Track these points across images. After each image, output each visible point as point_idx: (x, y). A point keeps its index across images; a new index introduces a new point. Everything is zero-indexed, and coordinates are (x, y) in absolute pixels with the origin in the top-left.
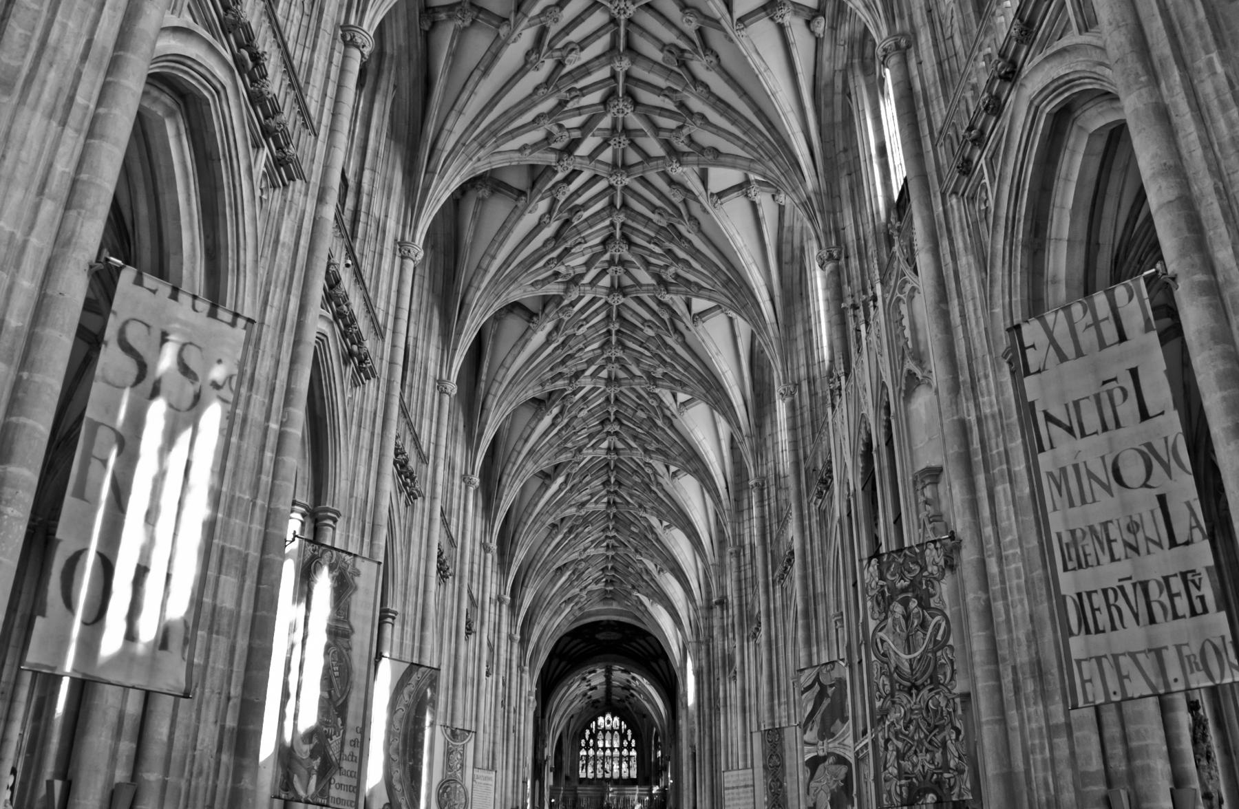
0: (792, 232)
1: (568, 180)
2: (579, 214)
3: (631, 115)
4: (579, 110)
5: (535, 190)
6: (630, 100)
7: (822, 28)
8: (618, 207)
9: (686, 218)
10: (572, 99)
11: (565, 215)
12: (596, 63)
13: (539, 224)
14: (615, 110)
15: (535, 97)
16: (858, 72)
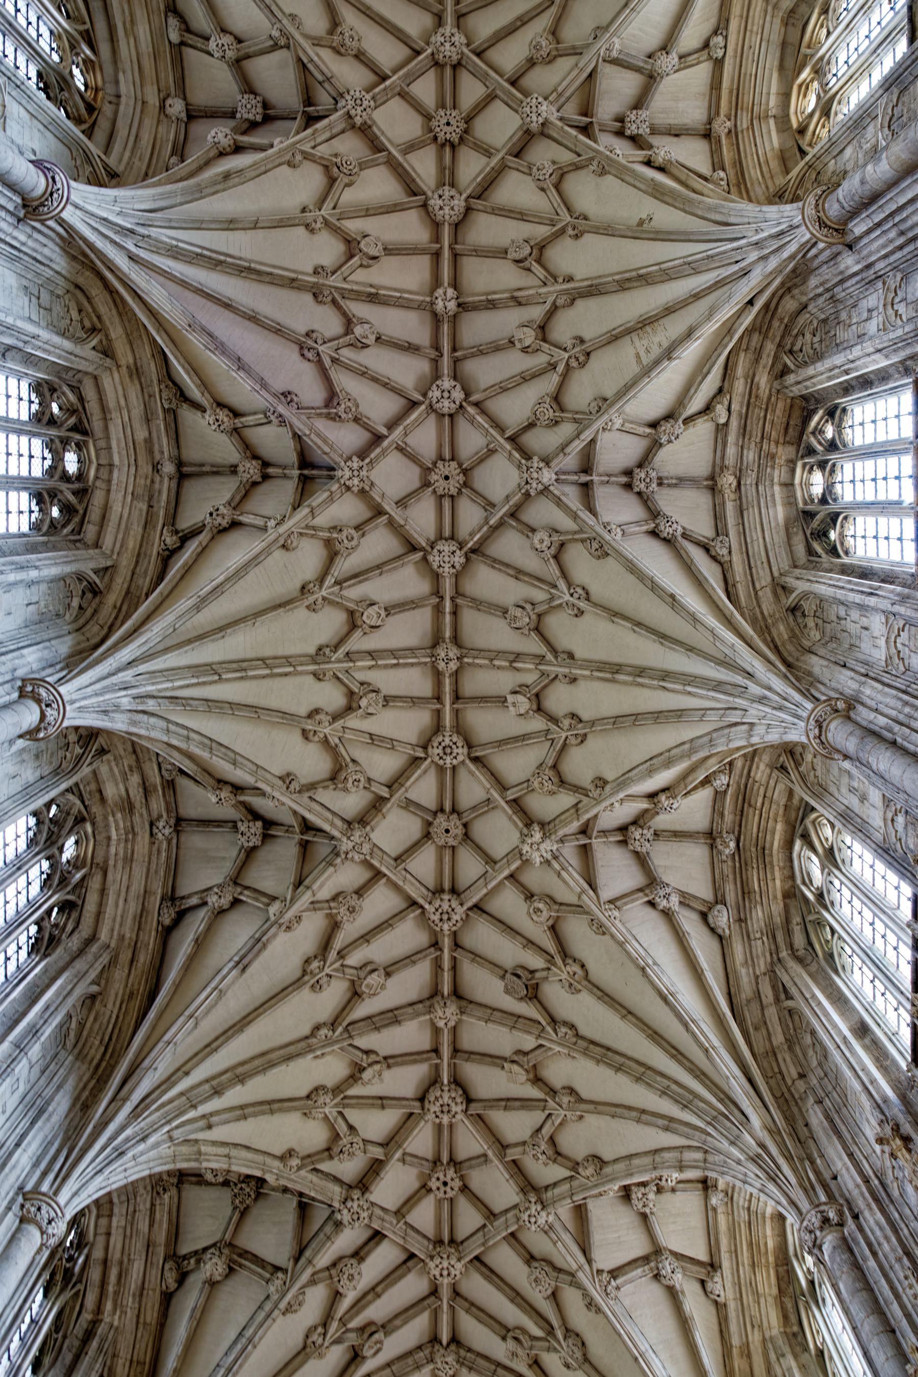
0: (749, 1356)
1: (359, 1254)
2: (376, 1337)
3: (460, 1116)
4: (382, 1102)
5: (303, 1261)
6: (460, 1092)
7: (725, 919)
8: (445, 1342)
9: (559, 1334)
10: (370, 1065)
11: (352, 1338)
12: (410, 1010)
13: (305, 1347)
14: (436, 1108)
15: (314, 1040)
16: (792, 964)
